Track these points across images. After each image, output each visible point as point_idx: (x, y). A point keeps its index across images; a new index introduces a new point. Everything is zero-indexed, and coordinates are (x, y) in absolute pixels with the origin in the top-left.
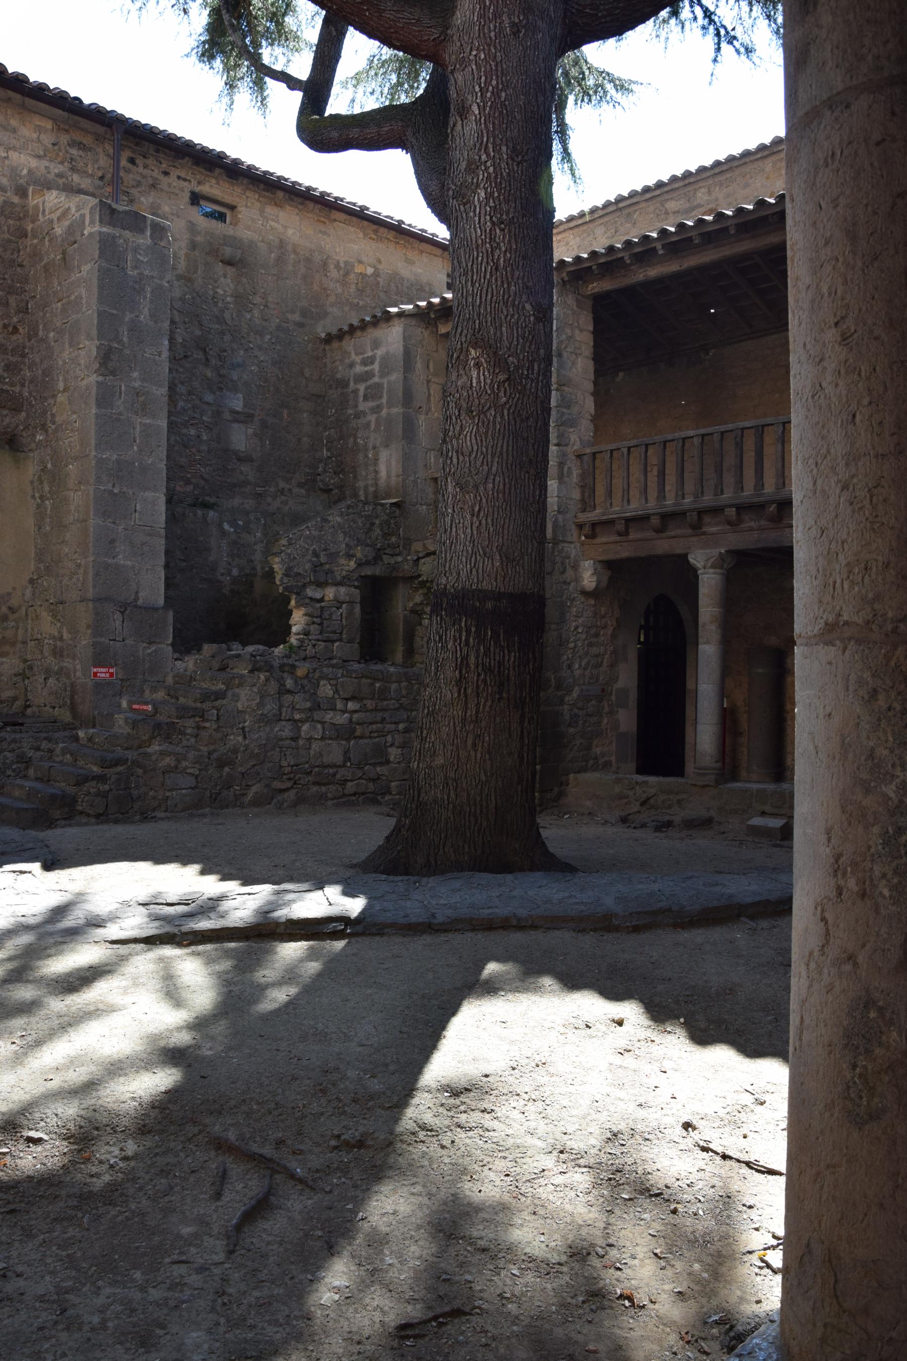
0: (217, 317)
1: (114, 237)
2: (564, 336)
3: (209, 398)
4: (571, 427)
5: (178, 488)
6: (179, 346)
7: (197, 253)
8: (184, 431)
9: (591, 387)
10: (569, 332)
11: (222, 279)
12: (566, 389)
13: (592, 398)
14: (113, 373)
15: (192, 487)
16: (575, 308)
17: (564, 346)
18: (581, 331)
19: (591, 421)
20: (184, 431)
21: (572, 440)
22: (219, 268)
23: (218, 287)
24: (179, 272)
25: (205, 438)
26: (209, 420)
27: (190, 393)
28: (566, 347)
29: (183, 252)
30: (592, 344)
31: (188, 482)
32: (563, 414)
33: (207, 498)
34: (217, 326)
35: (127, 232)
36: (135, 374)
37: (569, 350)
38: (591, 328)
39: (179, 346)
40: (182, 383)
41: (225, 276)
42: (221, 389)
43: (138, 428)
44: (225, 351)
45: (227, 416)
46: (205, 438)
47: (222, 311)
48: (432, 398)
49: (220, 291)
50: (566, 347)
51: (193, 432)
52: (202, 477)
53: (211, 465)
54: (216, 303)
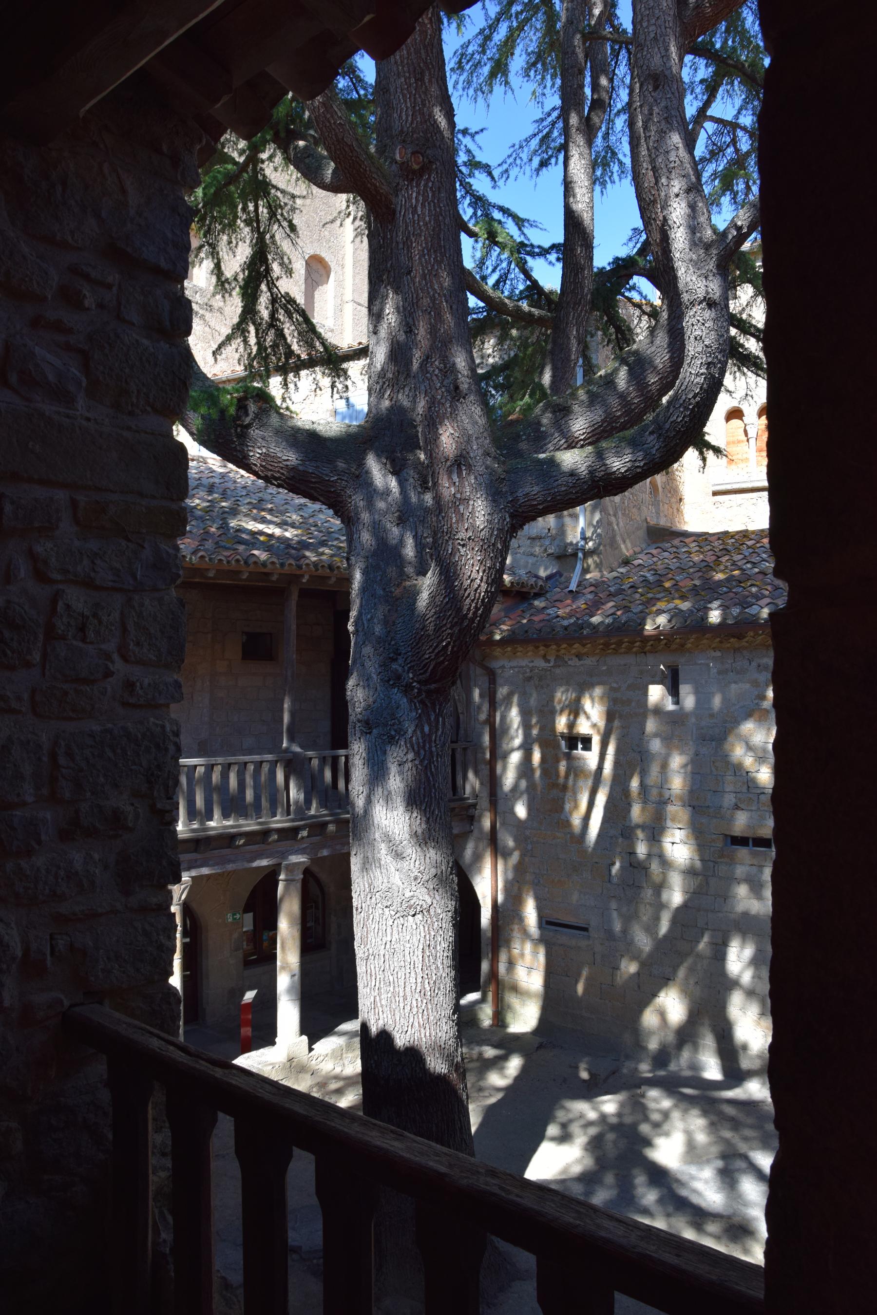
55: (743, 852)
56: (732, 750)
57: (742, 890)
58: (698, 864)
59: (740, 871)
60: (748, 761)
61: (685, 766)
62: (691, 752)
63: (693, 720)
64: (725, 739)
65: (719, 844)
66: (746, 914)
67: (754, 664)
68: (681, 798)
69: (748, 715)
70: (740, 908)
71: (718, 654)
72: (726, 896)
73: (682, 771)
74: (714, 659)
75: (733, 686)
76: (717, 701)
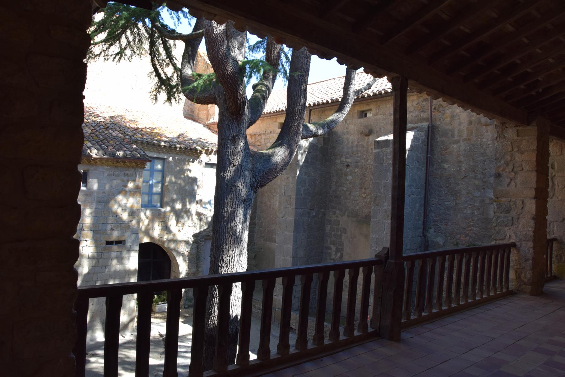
0: (482, 153)
1: (379, 153)
2: (502, 162)
3: (477, 194)
4: (506, 226)
5: (462, 238)
6: (463, 172)
7: (472, 126)
8: (465, 212)
9: (533, 193)
10: (508, 158)
11: (486, 134)
12: (503, 199)
13: (534, 201)
14: (377, 205)
15: (469, 237)
16: (515, 137)
17: (501, 170)
18: (522, 153)
19: (533, 218)
20: (465, 212)
21: (508, 236)
22: (484, 129)
23: (484, 138)
24: (464, 137)
25: (476, 214)
26: (477, 205)
27: (468, 193)
28: (504, 169)
29: (465, 128)
30: (535, 159)
31: (467, 235)
32: (498, 217)
33: (477, 243)
34: (482, 158)
35: (384, 149)
36: (385, 204)
37: (507, 170)
38: (534, 147)
39: (463, 172)
40: (464, 189)
41: (487, 132)
42: (484, 189)
43: (386, 225)
44: (486, 169)
45: (487, 201)
46: (476, 214)
47: (485, 150)
48: (556, 187)
49: (484, 140)
50: (504, 169)
51: (469, 211)
52: (474, 233)
53: (479, 227)
54: (482, 147)
55: (115, 247)
56: (112, 206)
57: (114, 262)
58: (95, 254)
59: (114, 254)
60: (119, 211)
61: (91, 213)
62: (94, 207)
63: (95, 194)
64: (109, 202)
65: (104, 245)
66: (115, 271)
67: (123, 173)
68: (88, 227)
69: (119, 193)
70: (113, 269)
71: (109, 168)
72: (107, 266)
73: (90, 215)
74: (107, 169)
75: (115, 181)
76: (107, 187)
